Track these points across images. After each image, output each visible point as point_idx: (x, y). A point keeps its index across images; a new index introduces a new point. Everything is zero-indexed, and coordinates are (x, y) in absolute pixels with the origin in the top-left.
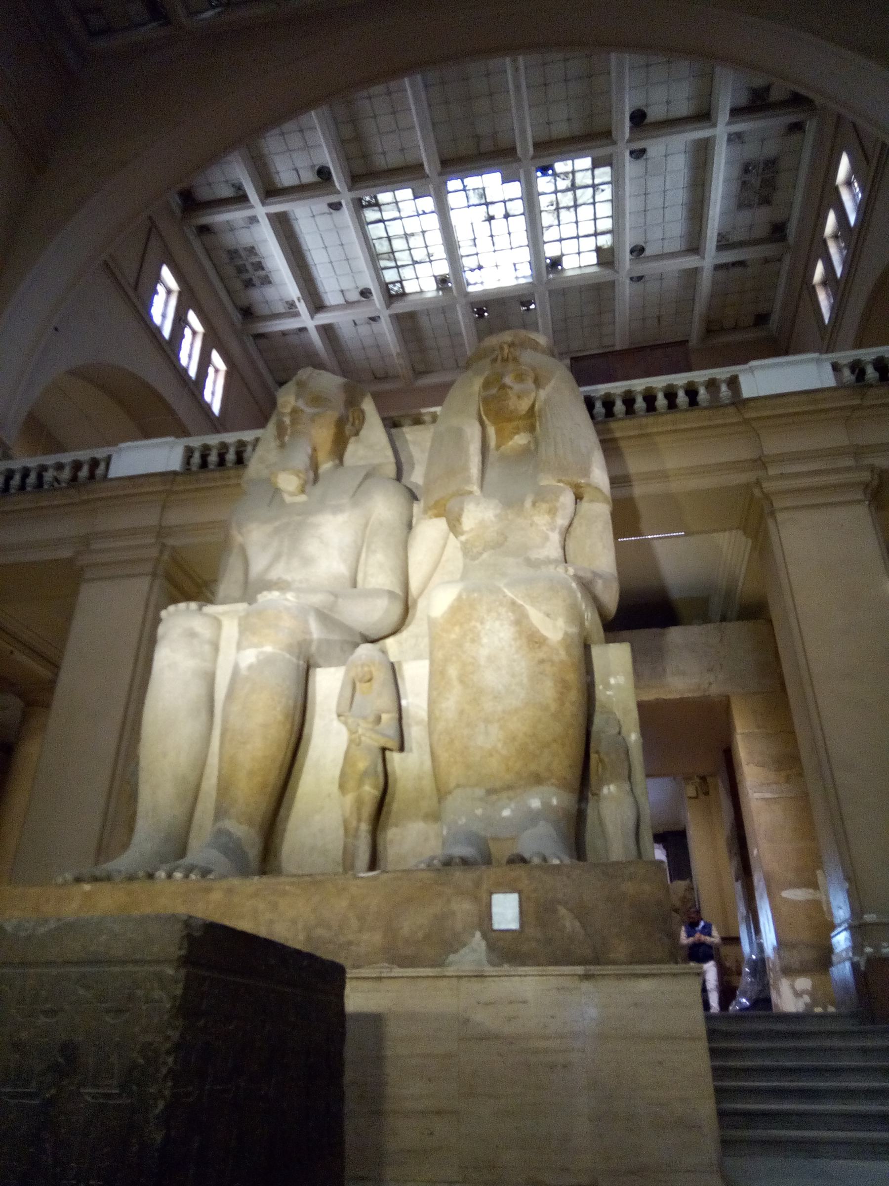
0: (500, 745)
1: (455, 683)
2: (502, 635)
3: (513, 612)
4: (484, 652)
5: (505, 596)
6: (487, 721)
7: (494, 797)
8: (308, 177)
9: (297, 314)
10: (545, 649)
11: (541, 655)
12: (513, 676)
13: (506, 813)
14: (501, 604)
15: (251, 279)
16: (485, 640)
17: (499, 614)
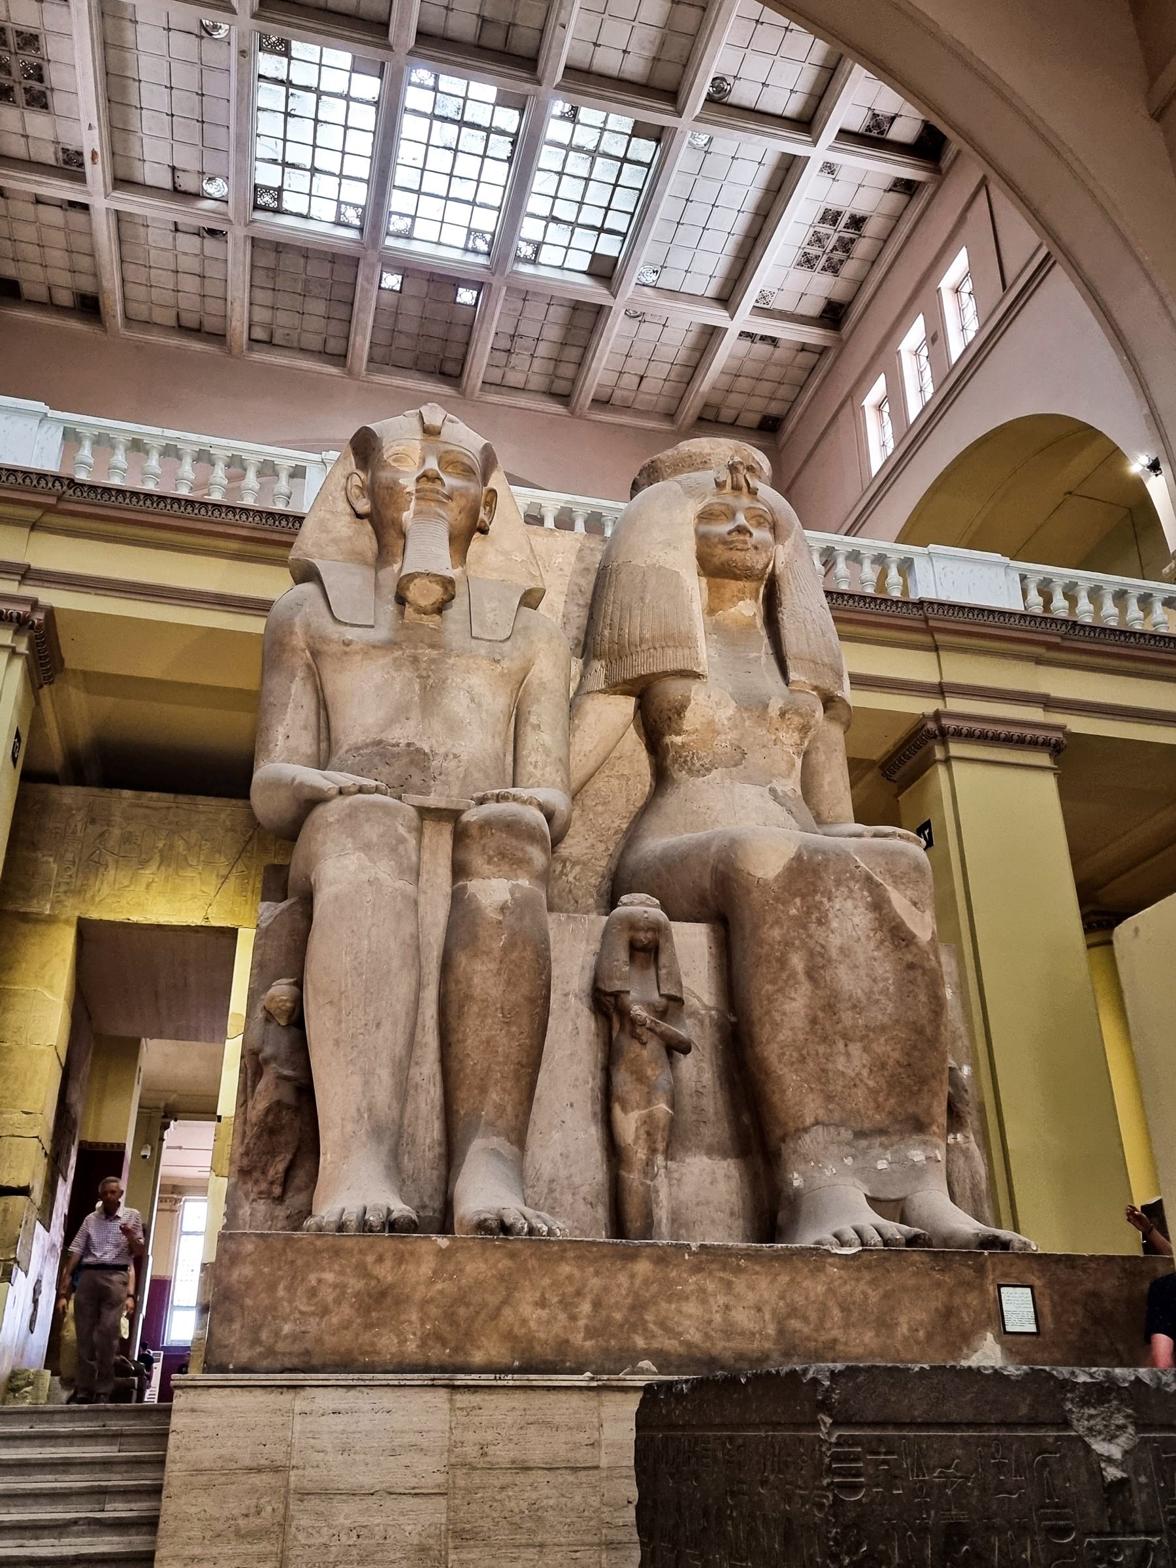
0: (865, 1072)
1: (802, 977)
2: (856, 920)
3: (871, 893)
4: (835, 941)
5: (857, 867)
6: (847, 1038)
7: (863, 1143)
10: (914, 949)
11: (909, 958)
12: (874, 980)
13: (882, 1165)
14: (852, 877)
15: (11, 89)
16: (835, 924)
17: (851, 891)
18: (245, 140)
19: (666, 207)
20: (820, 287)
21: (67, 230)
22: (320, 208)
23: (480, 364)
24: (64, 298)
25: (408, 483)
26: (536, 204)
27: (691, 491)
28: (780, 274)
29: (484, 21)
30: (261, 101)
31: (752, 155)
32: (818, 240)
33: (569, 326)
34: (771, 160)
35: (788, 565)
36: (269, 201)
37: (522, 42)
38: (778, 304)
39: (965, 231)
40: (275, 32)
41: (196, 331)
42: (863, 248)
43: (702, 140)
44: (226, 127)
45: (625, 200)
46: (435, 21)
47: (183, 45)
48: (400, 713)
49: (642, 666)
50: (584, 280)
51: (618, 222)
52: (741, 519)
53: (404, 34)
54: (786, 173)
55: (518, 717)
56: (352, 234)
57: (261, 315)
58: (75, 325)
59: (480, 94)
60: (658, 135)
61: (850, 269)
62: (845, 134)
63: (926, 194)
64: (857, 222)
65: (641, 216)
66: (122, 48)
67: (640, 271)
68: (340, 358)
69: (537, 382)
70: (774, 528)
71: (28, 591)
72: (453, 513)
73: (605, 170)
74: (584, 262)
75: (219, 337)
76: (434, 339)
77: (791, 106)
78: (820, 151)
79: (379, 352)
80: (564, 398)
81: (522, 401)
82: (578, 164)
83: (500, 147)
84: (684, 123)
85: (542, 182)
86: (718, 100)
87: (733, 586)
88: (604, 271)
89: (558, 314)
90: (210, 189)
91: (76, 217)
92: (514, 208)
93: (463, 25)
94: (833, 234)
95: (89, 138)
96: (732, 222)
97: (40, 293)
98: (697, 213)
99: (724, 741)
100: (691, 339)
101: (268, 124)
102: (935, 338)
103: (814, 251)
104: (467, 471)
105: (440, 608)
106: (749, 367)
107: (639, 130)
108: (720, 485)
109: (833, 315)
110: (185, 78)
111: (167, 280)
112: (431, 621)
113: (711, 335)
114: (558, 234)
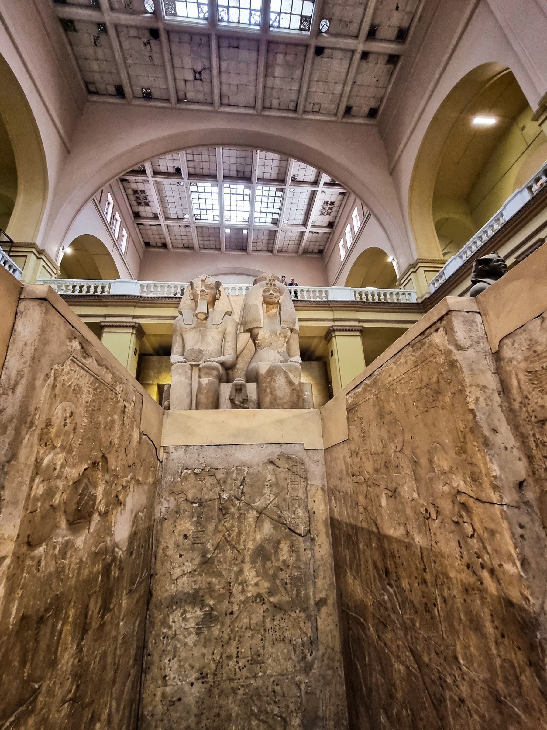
8: (171, 170)
9: (158, 219)
18: (190, 207)
19: (286, 206)
20: (326, 219)
21: (158, 230)
22: (210, 218)
23: (250, 247)
24: (159, 244)
25: (199, 293)
26: (257, 209)
27: (262, 286)
28: (316, 216)
29: (238, 171)
30: (192, 196)
31: (304, 192)
32: (324, 208)
33: (269, 235)
34: (309, 192)
35: (283, 300)
36: (198, 218)
37: (247, 175)
38: (317, 224)
39: (356, 204)
40: (193, 182)
41: (188, 248)
42: (335, 209)
43: (292, 190)
44: (185, 202)
45: (277, 206)
46: (227, 173)
47: (175, 188)
48: (197, 342)
49: (249, 327)
50: (271, 225)
51: (277, 211)
52: (271, 292)
53: (220, 177)
54: (313, 194)
55: (223, 340)
56: (217, 222)
57: (201, 242)
58: (162, 250)
59: (241, 187)
60: (282, 190)
61: (333, 214)
62: (325, 184)
63: (347, 195)
64: (332, 203)
65: (281, 209)
66: (162, 190)
67: (283, 220)
68: (219, 249)
69: (265, 249)
70: (280, 292)
71: (135, 320)
72: (209, 298)
73: (271, 200)
74: (270, 221)
75: (192, 248)
76: (240, 244)
77: (312, 179)
78: (320, 189)
79: (228, 247)
80: (271, 251)
81: (262, 253)
82: (265, 199)
83: (247, 198)
84: (287, 187)
85: (257, 205)
86: (294, 180)
87: (271, 306)
88: (275, 222)
89: (266, 233)
90: (185, 217)
91: (158, 227)
92: (252, 211)
93: (234, 173)
94: (327, 207)
95: (159, 211)
96: (303, 207)
97: (155, 244)
98: (294, 206)
99: (267, 342)
100: (298, 234)
101: (195, 201)
102: (352, 229)
103: (323, 211)
104: (212, 288)
105: (206, 319)
106: (313, 239)
107: (277, 190)
108: (267, 284)
109: (331, 225)
110: (176, 194)
111: (180, 238)
112: (204, 322)
113: (303, 233)
114: (263, 215)
